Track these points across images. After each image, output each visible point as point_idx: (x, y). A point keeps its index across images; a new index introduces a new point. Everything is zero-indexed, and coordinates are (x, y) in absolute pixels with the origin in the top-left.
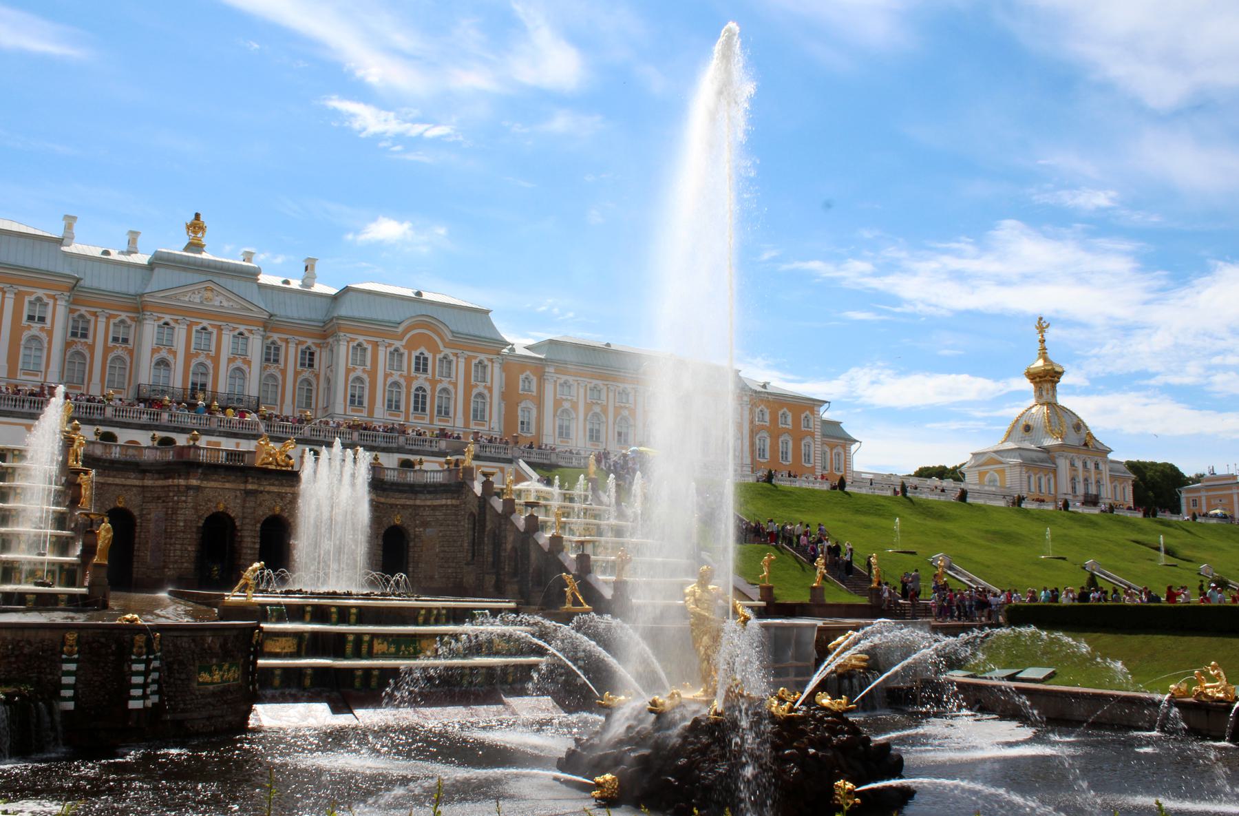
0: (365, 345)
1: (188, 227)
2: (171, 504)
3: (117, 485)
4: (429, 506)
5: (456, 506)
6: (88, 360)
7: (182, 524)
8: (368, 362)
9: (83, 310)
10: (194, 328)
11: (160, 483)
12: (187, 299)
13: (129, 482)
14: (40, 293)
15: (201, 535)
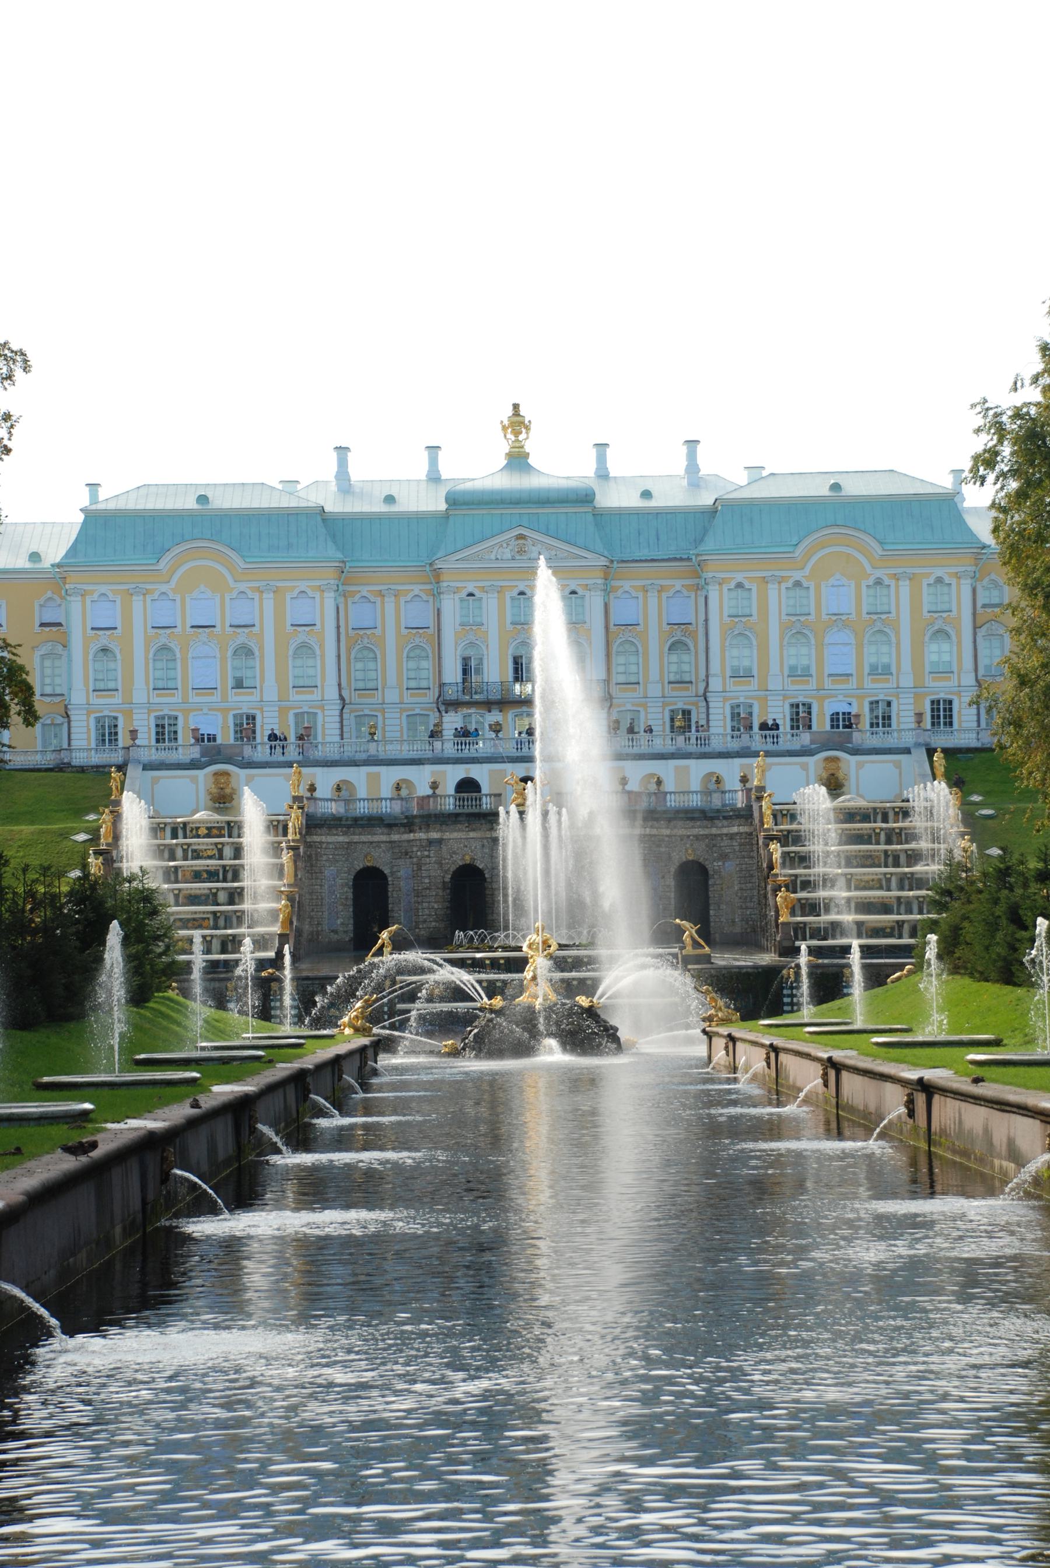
0: (747, 585)
1: (504, 428)
2: (415, 860)
3: (364, 843)
4: (726, 835)
5: (751, 834)
6: (379, 656)
7: (427, 881)
8: (755, 612)
9: (365, 594)
10: (508, 595)
11: (406, 837)
12: (493, 557)
13: (376, 838)
14: (303, 585)
15: (448, 891)
